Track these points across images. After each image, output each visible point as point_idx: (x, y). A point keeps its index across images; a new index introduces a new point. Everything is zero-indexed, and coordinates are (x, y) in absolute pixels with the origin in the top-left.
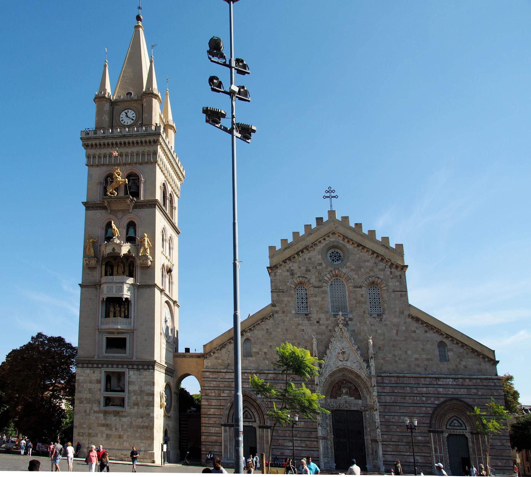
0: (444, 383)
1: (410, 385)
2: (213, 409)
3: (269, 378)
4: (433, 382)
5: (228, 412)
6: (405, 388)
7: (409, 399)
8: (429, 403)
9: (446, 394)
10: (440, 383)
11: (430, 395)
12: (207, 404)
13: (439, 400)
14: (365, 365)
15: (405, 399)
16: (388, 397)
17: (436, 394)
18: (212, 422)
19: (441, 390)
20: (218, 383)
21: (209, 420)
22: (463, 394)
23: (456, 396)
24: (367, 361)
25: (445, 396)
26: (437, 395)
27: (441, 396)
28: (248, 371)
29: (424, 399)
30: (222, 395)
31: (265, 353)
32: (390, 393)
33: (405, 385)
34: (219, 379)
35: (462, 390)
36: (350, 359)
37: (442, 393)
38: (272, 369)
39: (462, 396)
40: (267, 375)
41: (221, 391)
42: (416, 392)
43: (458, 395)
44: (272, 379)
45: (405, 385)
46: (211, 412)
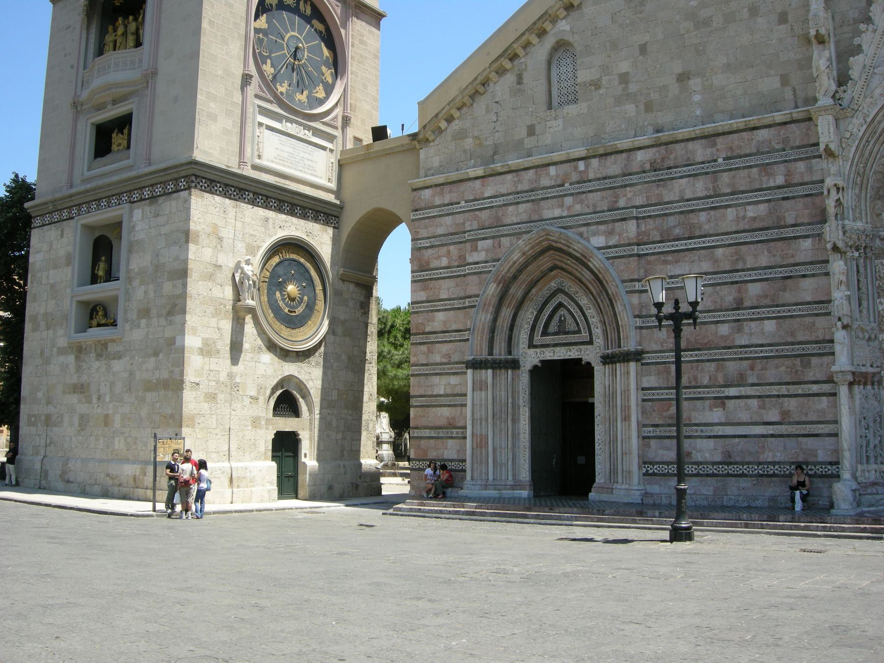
2: (441, 313)
3: (635, 168)
5: (489, 317)
12: (425, 299)
18: (437, 358)
20: (459, 218)
21: (430, 351)
28: (556, 156)
30: (470, 259)
31: (624, 79)
34: (463, 203)
40: (628, 158)
41: (468, 245)
44: (648, 166)
46: (436, 324)
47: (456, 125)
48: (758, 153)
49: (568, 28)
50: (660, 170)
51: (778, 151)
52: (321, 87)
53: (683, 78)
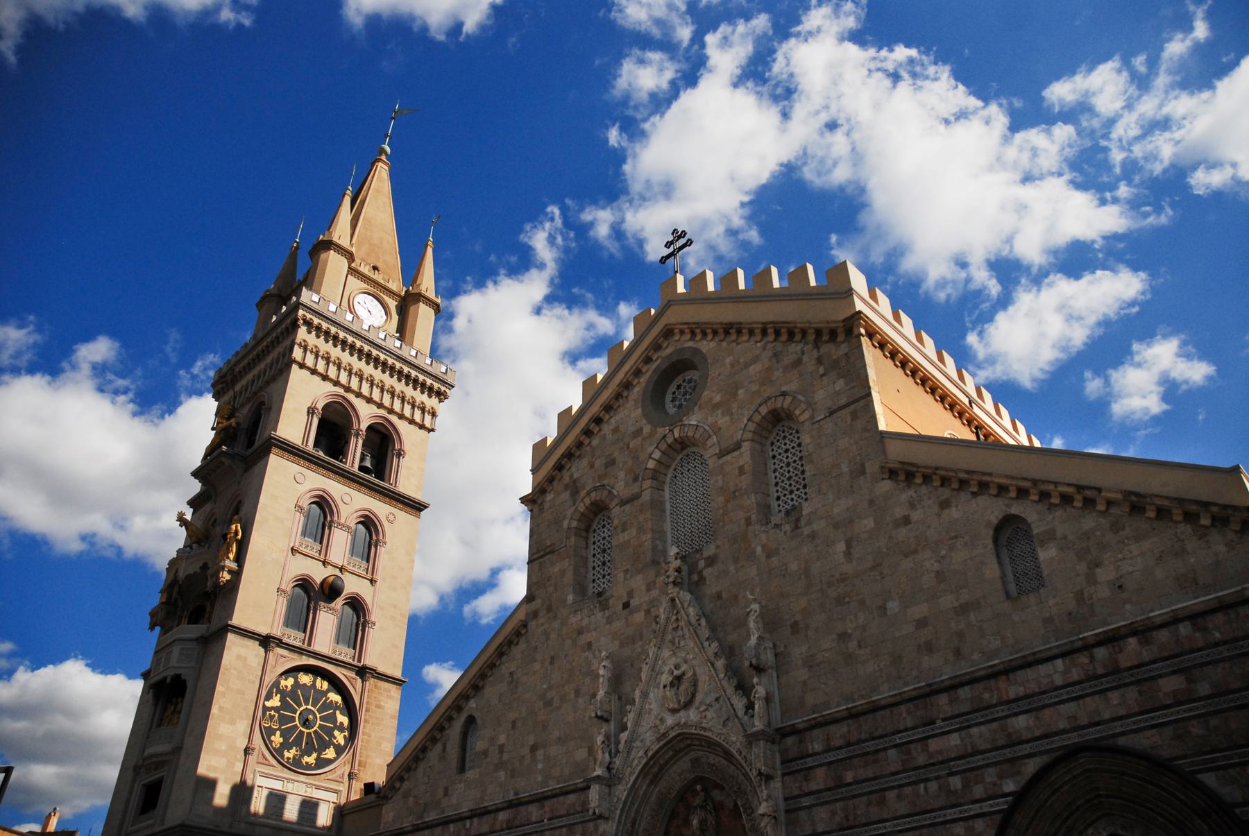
0: (1033, 688)
1: (898, 739)
4: (986, 695)
6: (881, 755)
7: (899, 797)
8: (978, 797)
9: (1046, 736)
10: (1014, 691)
11: (978, 760)
13: (1018, 773)
14: (739, 703)
15: (882, 802)
16: (819, 809)
17: (1003, 747)
19: (1021, 722)
22: (1122, 712)
23: (1093, 734)
24: (744, 688)
25: (1044, 745)
26: (1009, 754)
27: (1026, 749)
29: (956, 782)
31: (501, 748)
32: (829, 789)
33: (881, 744)
35: (1114, 697)
36: (699, 697)
37: (1029, 736)
38: (512, 793)
39: (1118, 727)
42: (921, 760)
43: (1097, 724)
44: (505, 826)
45: (881, 744)
47: (406, 785)
48: (568, 815)
49: (474, 706)
50: (511, 828)
51: (578, 813)
52: (332, 748)
53: (534, 749)
